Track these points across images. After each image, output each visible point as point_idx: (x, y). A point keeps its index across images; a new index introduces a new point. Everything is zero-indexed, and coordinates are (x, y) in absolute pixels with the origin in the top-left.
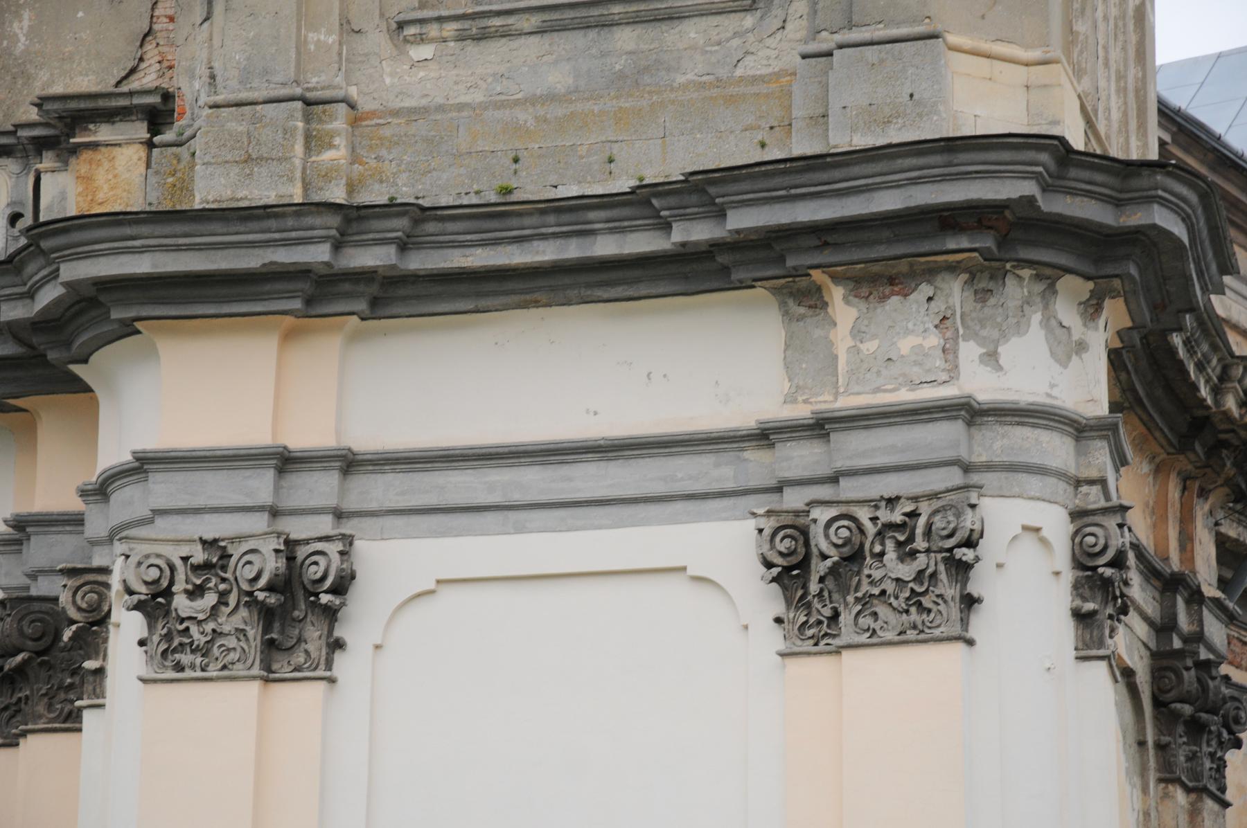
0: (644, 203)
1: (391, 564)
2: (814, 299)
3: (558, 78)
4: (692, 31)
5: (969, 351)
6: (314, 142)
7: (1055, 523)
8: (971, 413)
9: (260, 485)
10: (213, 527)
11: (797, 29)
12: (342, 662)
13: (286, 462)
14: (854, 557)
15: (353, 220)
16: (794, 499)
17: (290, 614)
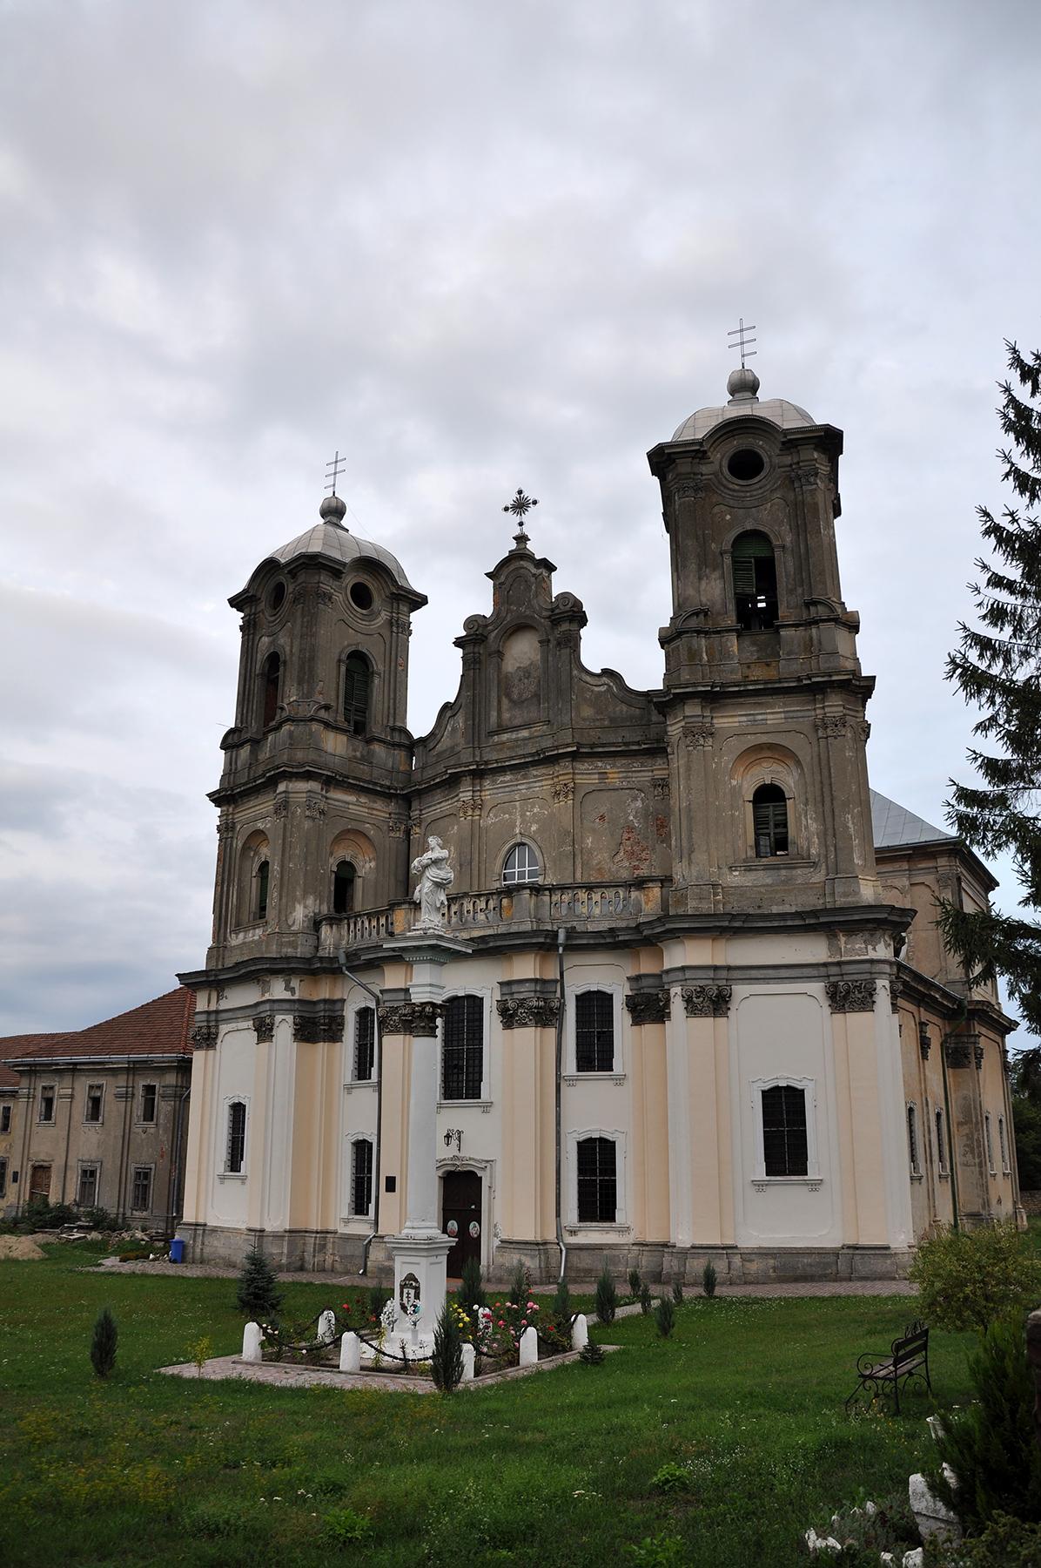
0: (798, 915)
1: (740, 990)
2: (836, 936)
3: (769, 881)
4: (799, 871)
6: (716, 894)
8: (872, 961)
9: (711, 974)
10: (702, 983)
11: (823, 872)
12: (730, 1013)
13: (716, 968)
14: (848, 992)
15: (733, 917)
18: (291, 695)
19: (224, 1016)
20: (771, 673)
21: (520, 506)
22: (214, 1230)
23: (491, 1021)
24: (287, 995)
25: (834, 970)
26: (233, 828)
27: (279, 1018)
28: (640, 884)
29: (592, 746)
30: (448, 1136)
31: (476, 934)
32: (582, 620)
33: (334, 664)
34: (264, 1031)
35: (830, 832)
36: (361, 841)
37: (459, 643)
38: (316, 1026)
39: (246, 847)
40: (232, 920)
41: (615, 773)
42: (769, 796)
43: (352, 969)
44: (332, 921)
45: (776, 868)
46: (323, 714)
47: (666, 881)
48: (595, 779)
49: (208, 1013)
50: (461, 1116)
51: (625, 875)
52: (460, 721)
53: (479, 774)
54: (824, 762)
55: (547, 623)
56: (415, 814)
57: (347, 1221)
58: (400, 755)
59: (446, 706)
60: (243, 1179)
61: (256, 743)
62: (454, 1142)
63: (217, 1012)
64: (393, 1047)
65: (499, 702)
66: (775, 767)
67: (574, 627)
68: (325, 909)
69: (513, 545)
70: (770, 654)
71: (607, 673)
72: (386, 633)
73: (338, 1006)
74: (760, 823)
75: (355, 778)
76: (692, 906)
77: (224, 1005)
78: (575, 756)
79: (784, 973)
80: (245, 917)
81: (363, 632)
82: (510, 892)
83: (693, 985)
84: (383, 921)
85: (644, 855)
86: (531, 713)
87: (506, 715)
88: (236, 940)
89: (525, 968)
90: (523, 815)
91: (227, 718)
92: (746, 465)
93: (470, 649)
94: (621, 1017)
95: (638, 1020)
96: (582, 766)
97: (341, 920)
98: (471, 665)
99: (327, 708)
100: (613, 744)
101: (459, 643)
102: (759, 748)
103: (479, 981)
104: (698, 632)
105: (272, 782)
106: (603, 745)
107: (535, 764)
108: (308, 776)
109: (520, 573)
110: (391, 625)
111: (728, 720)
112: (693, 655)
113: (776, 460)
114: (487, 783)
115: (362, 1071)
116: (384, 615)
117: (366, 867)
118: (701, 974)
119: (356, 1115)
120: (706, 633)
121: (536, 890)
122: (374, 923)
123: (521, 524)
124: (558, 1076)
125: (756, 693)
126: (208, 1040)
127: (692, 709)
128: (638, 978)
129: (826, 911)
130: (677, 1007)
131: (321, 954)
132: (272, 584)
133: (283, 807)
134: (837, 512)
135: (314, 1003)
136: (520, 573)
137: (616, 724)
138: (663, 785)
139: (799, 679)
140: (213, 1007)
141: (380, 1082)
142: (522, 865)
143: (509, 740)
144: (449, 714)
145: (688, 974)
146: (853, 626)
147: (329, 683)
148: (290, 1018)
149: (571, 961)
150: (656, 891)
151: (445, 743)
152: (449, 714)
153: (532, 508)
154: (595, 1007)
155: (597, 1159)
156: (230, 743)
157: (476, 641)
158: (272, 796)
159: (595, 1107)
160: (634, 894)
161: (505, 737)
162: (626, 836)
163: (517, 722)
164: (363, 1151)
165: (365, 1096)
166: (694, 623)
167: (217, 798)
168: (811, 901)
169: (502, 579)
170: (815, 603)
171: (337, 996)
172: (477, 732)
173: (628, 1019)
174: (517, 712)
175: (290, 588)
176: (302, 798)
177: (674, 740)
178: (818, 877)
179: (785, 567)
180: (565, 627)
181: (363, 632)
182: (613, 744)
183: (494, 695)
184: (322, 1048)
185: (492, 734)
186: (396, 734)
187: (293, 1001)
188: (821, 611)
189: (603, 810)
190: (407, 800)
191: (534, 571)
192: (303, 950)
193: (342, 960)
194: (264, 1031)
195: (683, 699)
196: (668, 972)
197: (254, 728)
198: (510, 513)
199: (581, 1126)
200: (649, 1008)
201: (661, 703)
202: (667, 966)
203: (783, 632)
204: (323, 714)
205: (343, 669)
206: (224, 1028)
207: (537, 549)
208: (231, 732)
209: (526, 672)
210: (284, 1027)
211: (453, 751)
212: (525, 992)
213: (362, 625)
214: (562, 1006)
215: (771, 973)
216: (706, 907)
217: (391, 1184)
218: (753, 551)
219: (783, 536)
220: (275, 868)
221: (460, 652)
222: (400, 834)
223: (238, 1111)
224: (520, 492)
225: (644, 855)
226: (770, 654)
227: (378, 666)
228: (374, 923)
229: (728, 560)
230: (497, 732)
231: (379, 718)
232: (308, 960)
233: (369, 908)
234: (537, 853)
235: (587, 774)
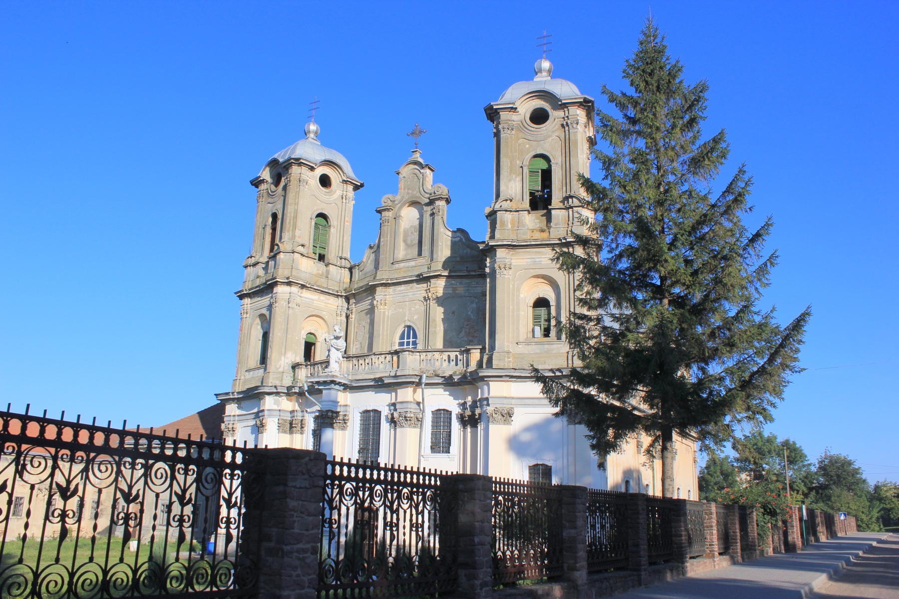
3: (538, 351)
46: (300, 249)
68: (300, 358)
72: (340, 203)
74: (536, 318)
75: (318, 286)
85: (476, 335)
90: (410, 310)
94: (456, 426)
104: (506, 211)
108: (289, 284)
116: (339, 193)
117: (322, 335)
139: (560, 239)
142: (408, 338)
149: (428, 392)
161: (402, 265)
162: (466, 323)
163: (409, 257)
170: (572, 197)
182: (461, 271)
204: (300, 249)
205: (313, 223)
225: (476, 335)
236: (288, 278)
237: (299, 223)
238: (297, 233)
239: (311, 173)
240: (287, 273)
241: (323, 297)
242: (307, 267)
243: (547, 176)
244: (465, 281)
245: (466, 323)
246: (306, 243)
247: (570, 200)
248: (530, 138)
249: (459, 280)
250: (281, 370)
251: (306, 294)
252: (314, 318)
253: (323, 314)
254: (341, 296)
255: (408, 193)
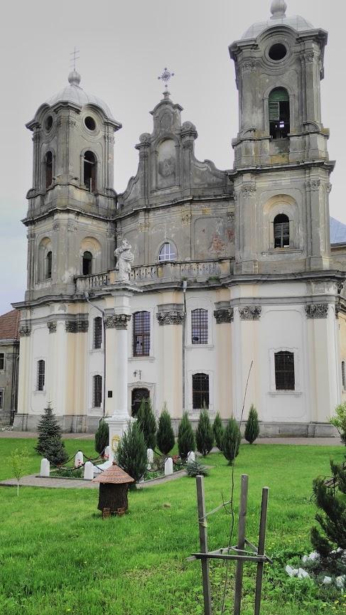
1: (265, 309)
3: (280, 259)
5: (326, 290)
7: (334, 306)
8: (326, 296)
9: (252, 301)
10: (247, 305)
16: (308, 304)
17: (256, 314)
18: (58, 172)
19: (32, 322)
20: (284, 160)
21: (166, 77)
22: (32, 416)
23: (154, 322)
24: (62, 312)
25: (308, 299)
26: (34, 236)
27: (59, 322)
28: (220, 261)
29: (199, 197)
30: (135, 373)
31: (146, 284)
32: (196, 136)
33: (78, 158)
34: (52, 328)
35: (310, 236)
36: (95, 242)
37: (138, 148)
38: (76, 326)
39: (41, 245)
40: (36, 278)
41: (208, 209)
42: (281, 219)
43: (92, 300)
44: (81, 278)
45: (284, 253)
46: (74, 182)
47: (232, 259)
48: (201, 213)
49: (26, 321)
50: (141, 363)
51: (214, 257)
52: (139, 185)
53: (147, 211)
54: (308, 203)
55: (179, 137)
56: (118, 230)
57: (91, 411)
58: (111, 202)
59: (132, 179)
60: (45, 395)
61: (43, 196)
62: (138, 375)
63: (30, 320)
64: (110, 334)
65: (156, 177)
66: (285, 206)
67: (192, 138)
68: (79, 272)
69: (163, 97)
70: (285, 149)
71: (207, 162)
72: (103, 141)
73: (86, 316)
75: (90, 213)
76: (244, 270)
77: (34, 317)
78: (191, 202)
79: (285, 301)
80: (42, 277)
81: (92, 141)
82: (161, 264)
83: (242, 307)
84: (105, 278)
86: (170, 181)
87: (160, 183)
88: (38, 287)
89: (169, 298)
91: (29, 184)
92: (277, 52)
93: (142, 150)
95: (219, 322)
96: (196, 206)
97: (86, 278)
98: (144, 157)
99: (76, 179)
100: (209, 196)
101: (138, 148)
102: (278, 196)
103: (150, 304)
104: (251, 140)
105: (52, 214)
106: (204, 197)
107: (173, 205)
108: (68, 211)
109: (165, 111)
110: (105, 138)
111: (263, 183)
112: (248, 152)
113: (293, 49)
114: (151, 214)
115: (97, 345)
116: (101, 134)
117: (97, 254)
118: (247, 301)
119: (94, 364)
120: (254, 140)
121: (174, 264)
122: (101, 279)
123: (166, 86)
124: (184, 347)
125: (277, 170)
126: (27, 332)
127: (247, 178)
128: (219, 303)
129: (305, 272)
130: (237, 315)
131: (77, 293)
132: (46, 117)
133: (56, 226)
134: (322, 77)
135: (75, 315)
136: (165, 111)
137: (211, 186)
138: (231, 215)
140: (28, 318)
141: (105, 350)
143: (161, 194)
144: (134, 182)
145: (242, 301)
146: (326, 136)
147: (76, 167)
148: (64, 322)
149: (190, 295)
150: (227, 264)
151: (132, 196)
152: (134, 182)
153: (172, 77)
154: (199, 314)
155: (201, 384)
156: (31, 196)
157: (146, 147)
158: (51, 221)
159: (200, 360)
160: (218, 265)
161: (159, 193)
162: (215, 239)
163: (165, 186)
164: (98, 380)
165: (98, 354)
166: (249, 135)
167: (28, 223)
168: (299, 268)
169: (157, 114)
170: (308, 124)
171: (86, 312)
172: (146, 192)
173: (215, 320)
174: (165, 181)
175: (55, 119)
176: (66, 222)
177: (237, 193)
178: (303, 257)
179: (294, 107)
180: (187, 138)
181: (92, 141)
182: (209, 196)
183: (154, 172)
184: (79, 335)
185: (152, 192)
186: (109, 192)
187: (66, 315)
188: (311, 129)
189: (204, 227)
190: (115, 222)
191: (173, 110)
192: (70, 291)
193: (87, 295)
194: (52, 328)
195: (241, 173)
196: (232, 300)
197: (42, 188)
198: (161, 80)
199: (195, 367)
200: (224, 316)
201: (233, 176)
202: (232, 297)
203: (292, 139)
206: (34, 327)
207: (174, 99)
208: (32, 190)
209: (169, 162)
210: (61, 326)
211: (135, 200)
212: (169, 309)
213: (91, 138)
214: (185, 316)
215: (280, 301)
216: (250, 271)
217: (110, 394)
218: (279, 98)
219: (294, 91)
220: (54, 255)
221: (138, 151)
222: (113, 239)
223: (41, 363)
224: (166, 69)
225: (223, 248)
226: (285, 149)
227: (100, 158)
228: (101, 279)
229: (266, 102)
230: (155, 191)
231: (101, 184)
232: (72, 296)
233: (99, 273)
234: (174, 247)
235: (198, 210)
236: (65, 206)
237: (71, 160)
238: (70, 168)
239: (77, 116)
240: (64, 202)
241: (95, 222)
242: (81, 197)
243: (285, 108)
244: (213, 204)
245: (215, 239)
246: (79, 177)
247: (307, 127)
248: (270, 73)
249: (208, 204)
250: (65, 282)
251: (82, 220)
252: (89, 240)
253: (96, 236)
254: (110, 221)
255: (161, 131)
